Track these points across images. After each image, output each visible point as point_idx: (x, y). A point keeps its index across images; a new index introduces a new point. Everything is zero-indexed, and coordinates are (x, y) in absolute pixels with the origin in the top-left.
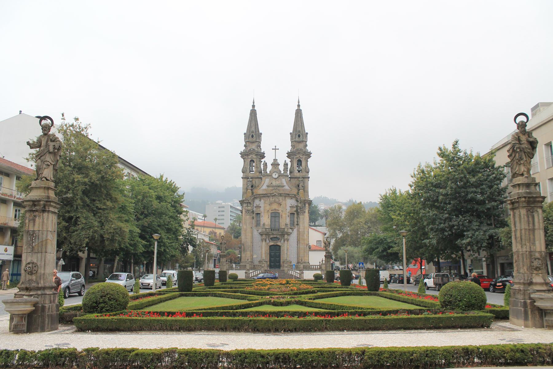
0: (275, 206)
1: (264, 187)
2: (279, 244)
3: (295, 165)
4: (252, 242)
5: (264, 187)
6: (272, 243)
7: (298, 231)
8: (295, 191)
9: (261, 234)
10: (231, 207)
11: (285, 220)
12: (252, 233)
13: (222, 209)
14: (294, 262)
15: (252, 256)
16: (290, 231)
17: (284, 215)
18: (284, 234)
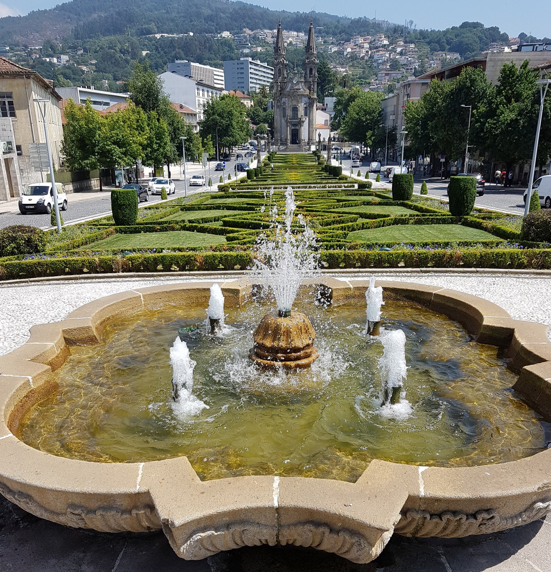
0: (295, 103)
1: (288, 89)
2: (297, 128)
3: (308, 72)
4: (281, 127)
5: (288, 89)
6: (293, 128)
7: (309, 119)
8: (308, 91)
9: (287, 122)
10: (250, 62)
11: (301, 112)
12: (281, 120)
13: (242, 66)
14: (307, 140)
15: (281, 136)
16: (304, 119)
17: (300, 109)
18: (300, 123)
